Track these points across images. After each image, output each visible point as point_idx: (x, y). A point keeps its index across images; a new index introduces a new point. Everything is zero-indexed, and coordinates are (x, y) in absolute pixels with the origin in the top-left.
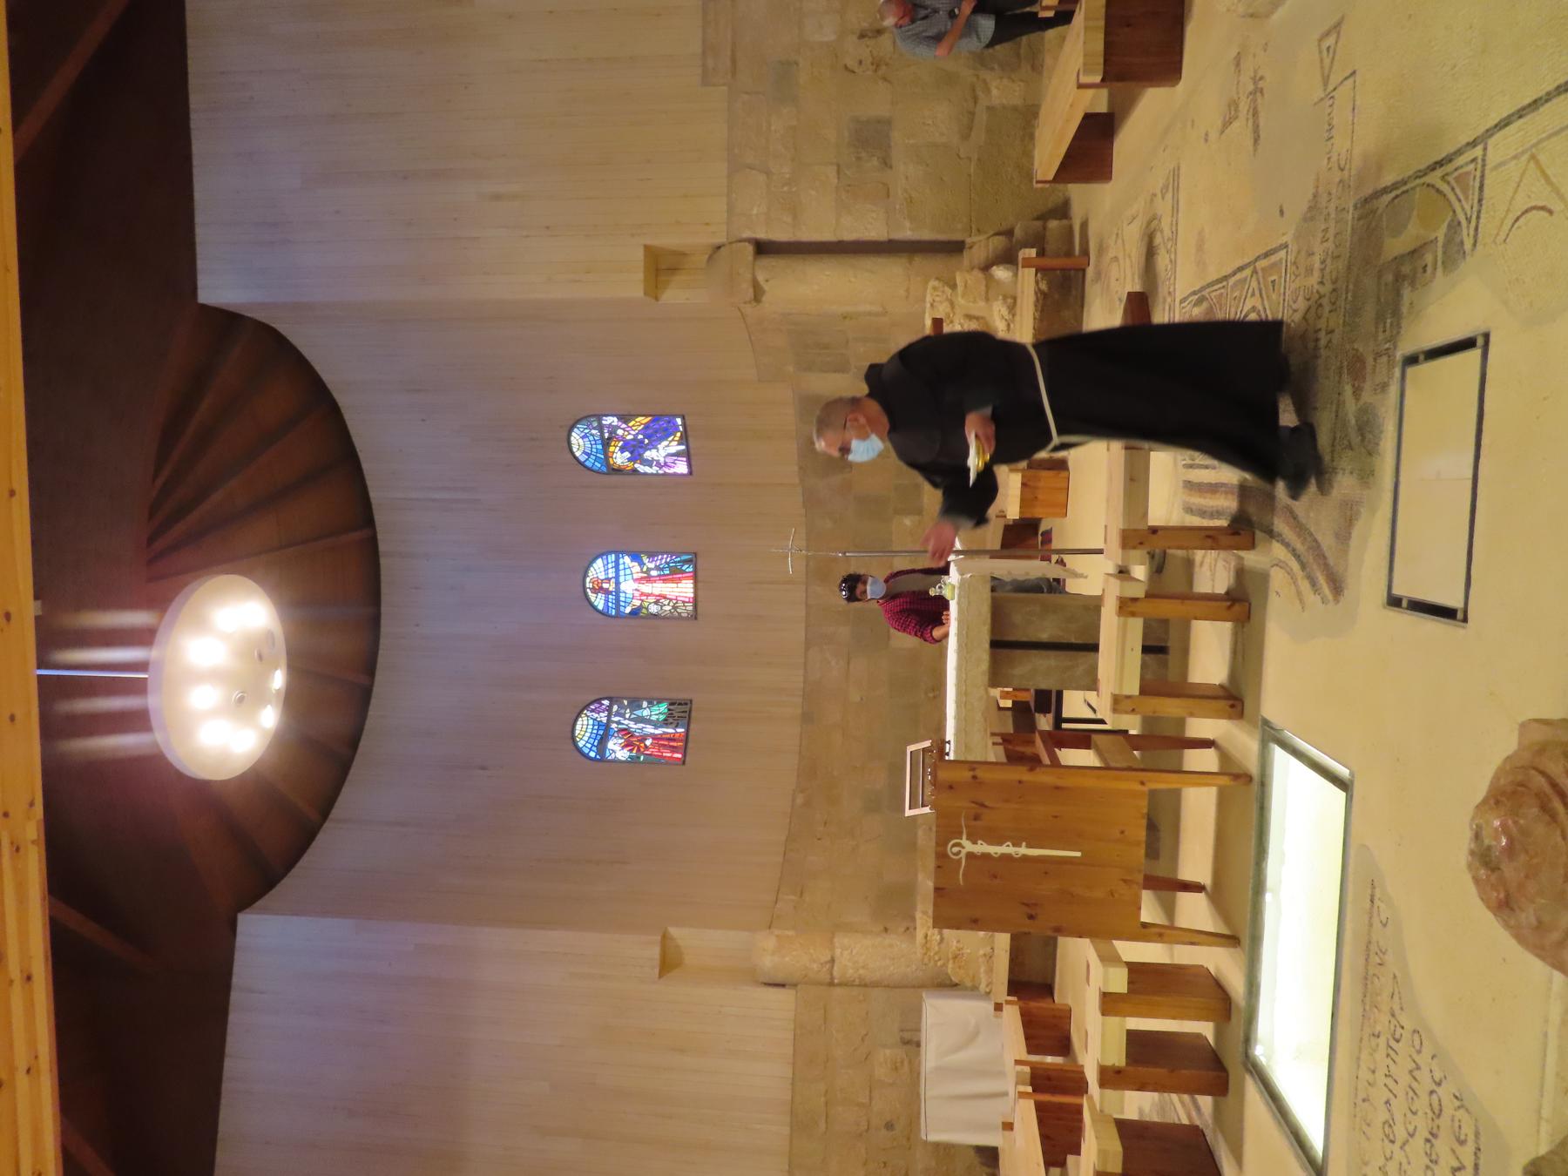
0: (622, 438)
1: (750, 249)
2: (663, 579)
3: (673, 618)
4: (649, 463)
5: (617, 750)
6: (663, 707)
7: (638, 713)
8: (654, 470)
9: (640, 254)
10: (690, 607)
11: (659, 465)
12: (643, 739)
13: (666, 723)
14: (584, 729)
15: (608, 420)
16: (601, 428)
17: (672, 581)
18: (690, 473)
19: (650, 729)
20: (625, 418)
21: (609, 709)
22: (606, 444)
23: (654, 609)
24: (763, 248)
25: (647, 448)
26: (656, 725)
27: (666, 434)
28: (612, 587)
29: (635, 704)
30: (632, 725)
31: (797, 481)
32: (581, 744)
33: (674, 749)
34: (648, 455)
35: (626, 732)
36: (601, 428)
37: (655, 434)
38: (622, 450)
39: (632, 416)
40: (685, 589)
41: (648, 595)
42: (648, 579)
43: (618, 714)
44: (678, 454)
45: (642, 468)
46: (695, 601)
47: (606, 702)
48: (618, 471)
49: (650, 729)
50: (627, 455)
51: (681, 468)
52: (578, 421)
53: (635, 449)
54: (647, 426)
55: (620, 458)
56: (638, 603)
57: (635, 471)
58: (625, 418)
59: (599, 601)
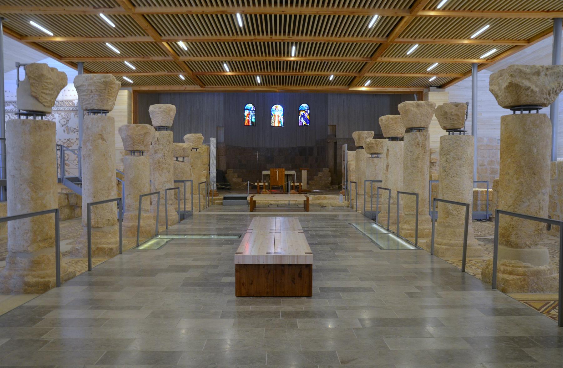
0: (305, 114)
1: (335, 141)
2: (279, 120)
3: (270, 122)
4: (301, 118)
5: (246, 112)
6: (254, 121)
7: (253, 116)
8: (300, 119)
9: (335, 124)
10: (273, 125)
11: (301, 120)
12: (249, 117)
13: (251, 121)
14: (250, 106)
15: (309, 111)
16: (307, 110)
17: (278, 122)
18: (299, 126)
19: (250, 118)
20: (309, 115)
21: (254, 110)
22: (304, 110)
23: (273, 118)
24: (336, 143)
25: (304, 118)
26: (251, 119)
27: (306, 122)
28: (277, 110)
29: (255, 115)
30: (251, 115)
31: (298, 146)
32: (247, 105)
33: (247, 123)
34: (302, 118)
35: (250, 114)
36: (307, 110)
37: (306, 120)
38: (303, 114)
39: (309, 116)
40: (277, 125)
41: (275, 117)
42: (278, 117)
43: (253, 112)
44: (303, 124)
45: (300, 117)
46: (274, 126)
47: (255, 109)
48: (299, 113)
49: (250, 118)
50: (302, 114)
51: (300, 124)
52: (309, 106)
53: (303, 116)
54: (308, 119)
55: (302, 113)
56: (274, 115)
57: (299, 115)
58: (309, 115)
59: (274, 107)
